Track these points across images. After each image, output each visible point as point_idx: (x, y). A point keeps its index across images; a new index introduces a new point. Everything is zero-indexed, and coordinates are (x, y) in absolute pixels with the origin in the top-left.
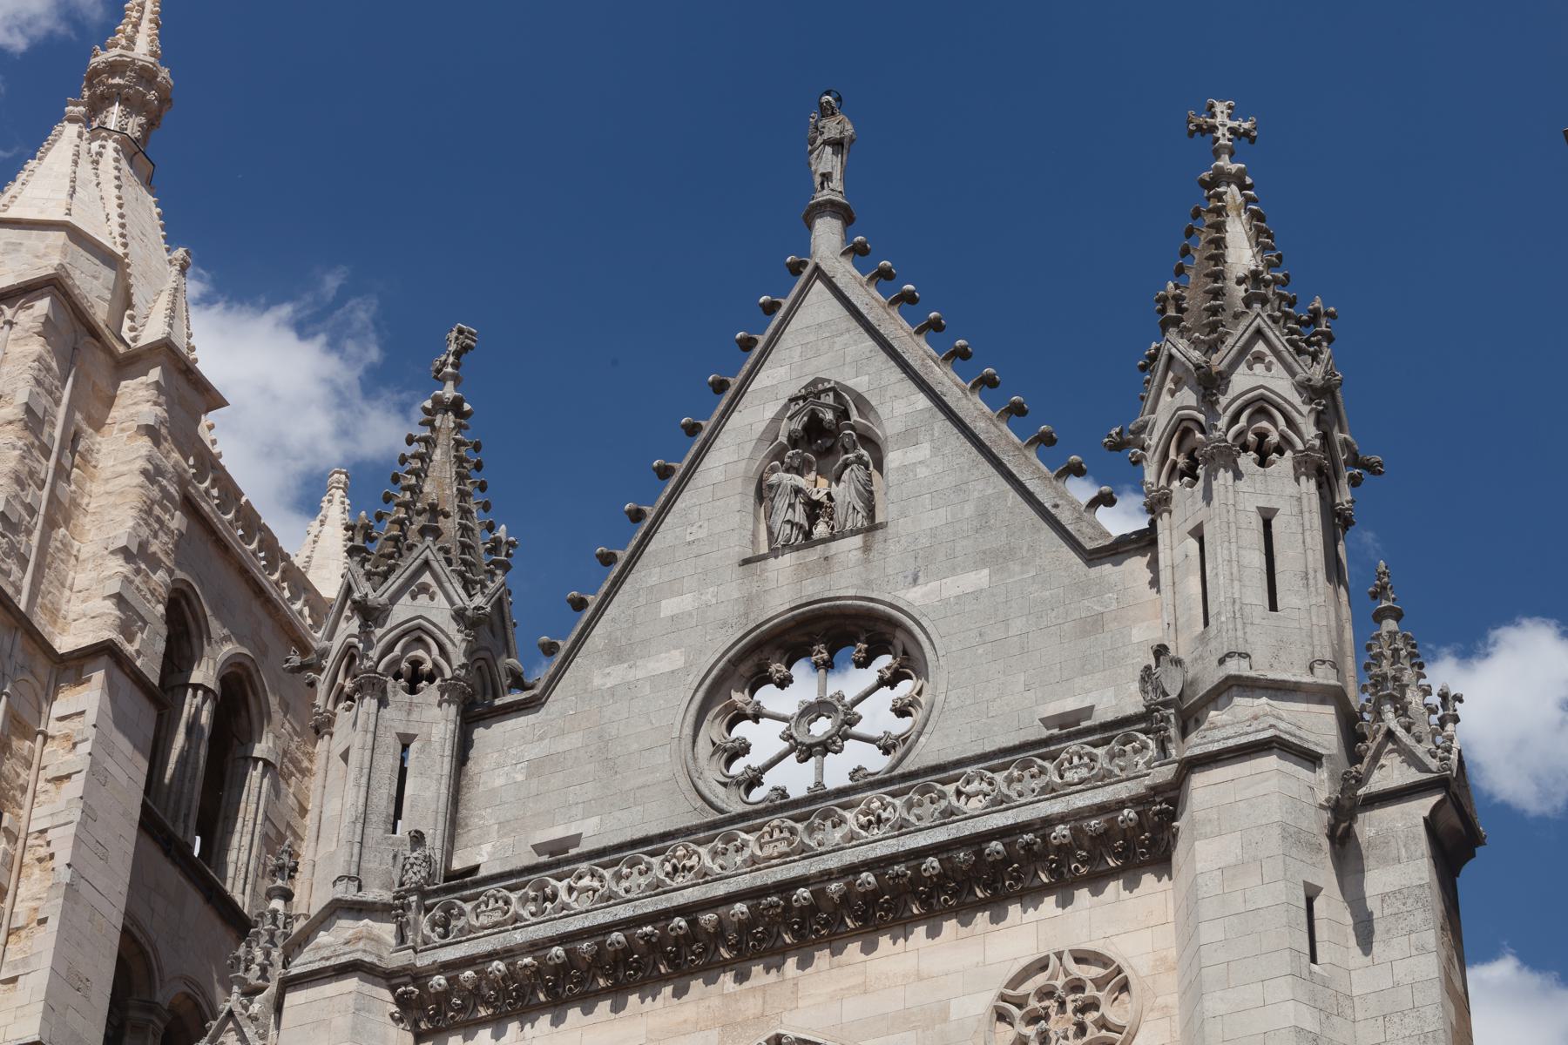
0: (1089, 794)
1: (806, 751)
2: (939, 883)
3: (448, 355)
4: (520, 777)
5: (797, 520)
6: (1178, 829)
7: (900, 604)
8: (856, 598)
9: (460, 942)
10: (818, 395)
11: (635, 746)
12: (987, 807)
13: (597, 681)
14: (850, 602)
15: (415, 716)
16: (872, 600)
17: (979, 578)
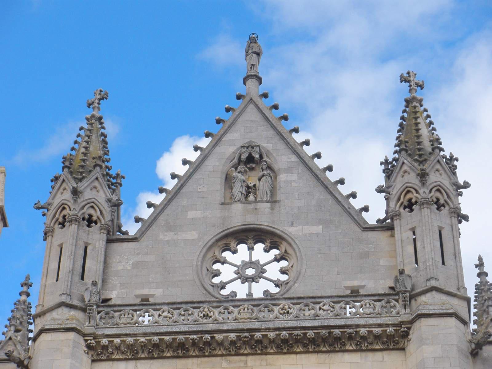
0: (375, 319)
1: (245, 279)
2: (312, 341)
3: (96, 99)
4: (129, 268)
5: (243, 192)
6: (411, 339)
7: (286, 232)
8: (268, 226)
9: (114, 327)
10: (253, 147)
11: (178, 265)
12: (332, 316)
13: (161, 237)
14: (265, 227)
15: (90, 236)
16: (274, 228)
17: (318, 229)
